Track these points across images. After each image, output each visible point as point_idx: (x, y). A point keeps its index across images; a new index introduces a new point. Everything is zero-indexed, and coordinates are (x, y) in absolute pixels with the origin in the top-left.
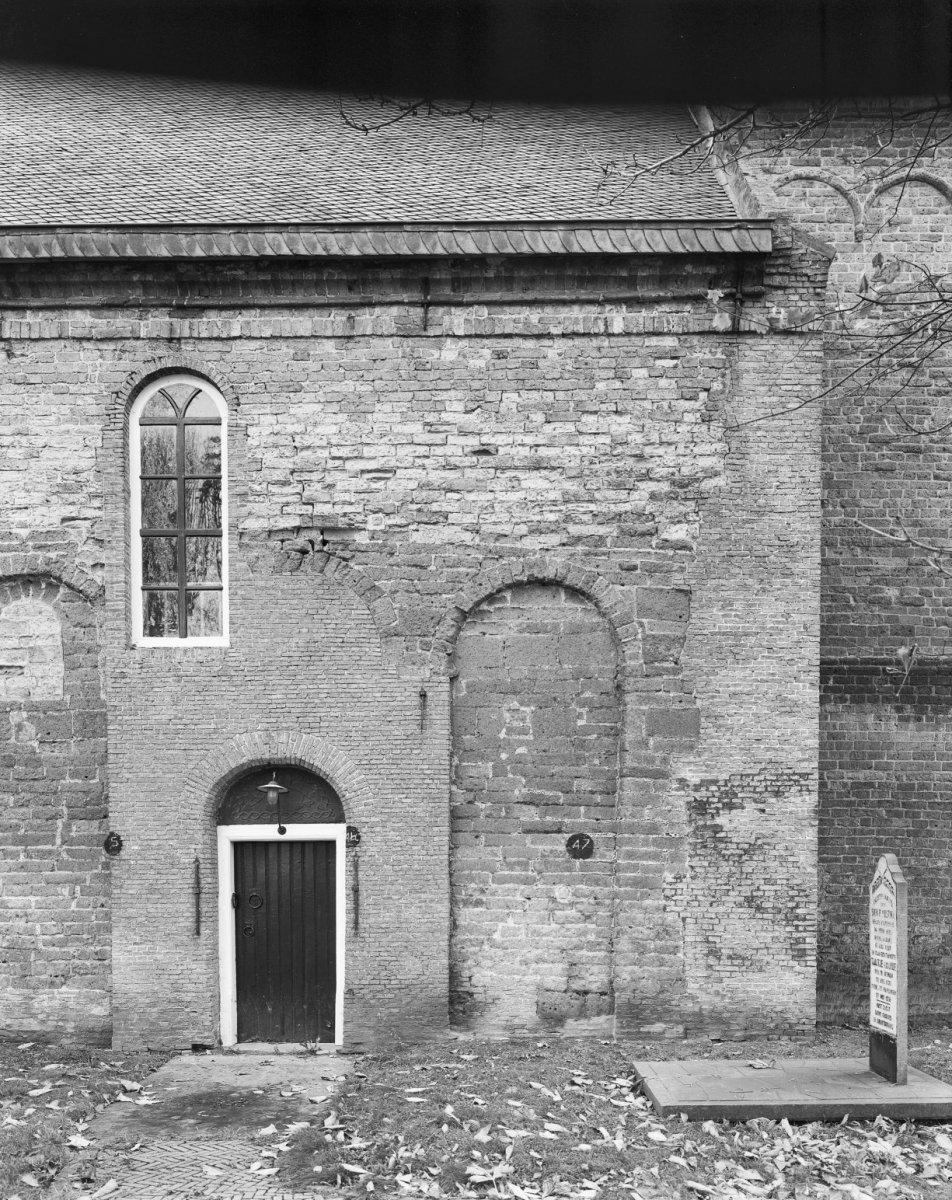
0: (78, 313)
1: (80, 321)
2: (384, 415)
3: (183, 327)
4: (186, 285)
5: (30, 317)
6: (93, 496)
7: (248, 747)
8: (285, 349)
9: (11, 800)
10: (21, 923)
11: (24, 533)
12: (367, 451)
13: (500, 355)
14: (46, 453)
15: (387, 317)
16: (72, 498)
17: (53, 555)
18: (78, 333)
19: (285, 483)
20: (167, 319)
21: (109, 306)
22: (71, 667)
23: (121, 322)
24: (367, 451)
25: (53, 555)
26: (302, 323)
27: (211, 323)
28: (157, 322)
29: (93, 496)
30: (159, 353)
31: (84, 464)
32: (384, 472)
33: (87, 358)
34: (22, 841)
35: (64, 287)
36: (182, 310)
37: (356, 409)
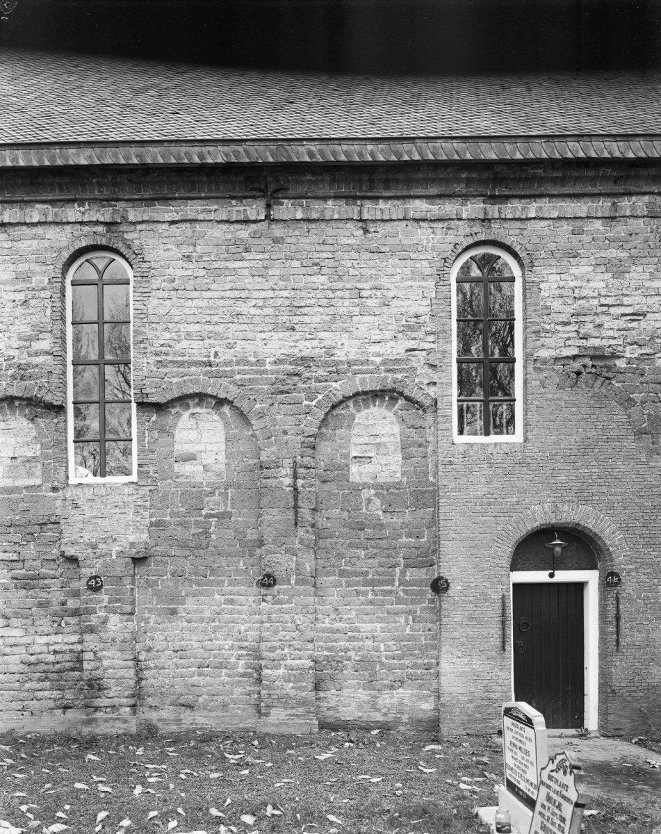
0: (417, 202)
1: (419, 207)
2: (637, 274)
3: (494, 211)
4: (498, 180)
5: (381, 204)
6: (429, 333)
7: (540, 514)
8: (566, 227)
9: (362, 553)
10: (369, 643)
11: (378, 360)
12: (626, 300)
14: (394, 303)
15: (641, 203)
16: (414, 335)
17: (399, 376)
18: (417, 216)
19: (568, 324)
20: (482, 205)
21: (440, 196)
22: (407, 457)
24: (626, 300)
25: (399, 376)
27: (513, 208)
28: (474, 208)
29: (429, 333)
30: (475, 229)
31: (422, 310)
32: (638, 315)
33: (423, 234)
34: (371, 583)
35: (409, 182)
36: (493, 199)
37: (617, 269)
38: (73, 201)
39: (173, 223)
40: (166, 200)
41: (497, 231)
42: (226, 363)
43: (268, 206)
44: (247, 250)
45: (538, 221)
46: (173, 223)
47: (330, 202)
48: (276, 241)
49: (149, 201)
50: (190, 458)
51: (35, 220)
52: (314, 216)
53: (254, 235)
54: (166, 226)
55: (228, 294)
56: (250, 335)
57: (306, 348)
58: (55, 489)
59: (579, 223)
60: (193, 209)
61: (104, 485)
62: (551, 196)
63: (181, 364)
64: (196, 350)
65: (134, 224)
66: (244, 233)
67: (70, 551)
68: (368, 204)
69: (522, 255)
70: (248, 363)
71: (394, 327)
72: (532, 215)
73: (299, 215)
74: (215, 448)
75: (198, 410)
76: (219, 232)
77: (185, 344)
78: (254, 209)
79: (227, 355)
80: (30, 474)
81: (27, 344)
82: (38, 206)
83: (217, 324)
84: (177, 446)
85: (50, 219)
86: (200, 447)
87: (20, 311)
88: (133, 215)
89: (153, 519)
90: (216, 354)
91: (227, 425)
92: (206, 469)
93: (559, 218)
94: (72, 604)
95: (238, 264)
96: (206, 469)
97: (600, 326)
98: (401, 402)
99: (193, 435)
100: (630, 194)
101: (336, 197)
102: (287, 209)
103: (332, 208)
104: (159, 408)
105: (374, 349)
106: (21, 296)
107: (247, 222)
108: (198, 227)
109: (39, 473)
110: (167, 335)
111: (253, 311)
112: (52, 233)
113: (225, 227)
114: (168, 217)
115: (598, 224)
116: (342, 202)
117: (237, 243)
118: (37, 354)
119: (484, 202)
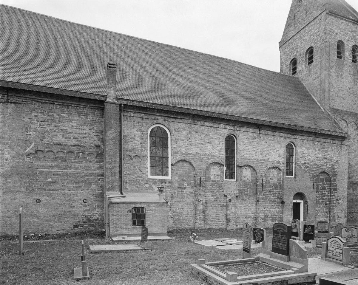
0: (281, 133)
1: (282, 134)
3: (292, 136)
4: (293, 132)
8: (301, 141)
11: (275, 161)
13: (321, 144)
14: (278, 151)
16: (281, 157)
20: (290, 135)
21: (285, 133)
23: (286, 135)
26: (304, 138)
28: (289, 136)
31: (282, 153)
35: (281, 130)
36: (292, 134)
37: (308, 149)
38: (228, 125)
39: (244, 131)
40: (243, 127)
41: (294, 141)
42: (253, 160)
43: (259, 131)
44: (256, 138)
45: (298, 140)
46: (244, 131)
48: (260, 137)
49: (240, 127)
50: (245, 177)
51: (221, 127)
52: (266, 134)
53: (257, 135)
54: (243, 132)
55: (253, 146)
57: (265, 158)
58: (222, 181)
60: (248, 129)
61: (230, 181)
63: (245, 159)
64: (247, 156)
65: (238, 130)
66: (255, 135)
67: (226, 194)
68: (274, 133)
69: (296, 145)
70: (256, 160)
71: (278, 156)
72: (297, 138)
73: (264, 133)
74: (249, 175)
75: (247, 168)
76: (251, 134)
77: (246, 155)
78: (257, 131)
79: (252, 158)
80: (218, 178)
81: (219, 152)
82: (221, 125)
85: (224, 127)
87: (218, 145)
88: (238, 129)
89: (239, 188)
90: (251, 158)
91: (251, 171)
92: (248, 179)
94: (225, 204)
95: (254, 141)
96: (248, 179)
97: (306, 158)
98: (277, 169)
99: (246, 172)
100: (310, 137)
102: (262, 131)
103: (269, 132)
104: (240, 167)
106: (218, 142)
107: (256, 133)
108: (248, 133)
109: (219, 178)
110: (243, 153)
111: (257, 150)
112: (224, 130)
113: (252, 133)
114: (244, 130)
115: (306, 141)
116: (270, 132)
117: (254, 137)
118: (221, 154)
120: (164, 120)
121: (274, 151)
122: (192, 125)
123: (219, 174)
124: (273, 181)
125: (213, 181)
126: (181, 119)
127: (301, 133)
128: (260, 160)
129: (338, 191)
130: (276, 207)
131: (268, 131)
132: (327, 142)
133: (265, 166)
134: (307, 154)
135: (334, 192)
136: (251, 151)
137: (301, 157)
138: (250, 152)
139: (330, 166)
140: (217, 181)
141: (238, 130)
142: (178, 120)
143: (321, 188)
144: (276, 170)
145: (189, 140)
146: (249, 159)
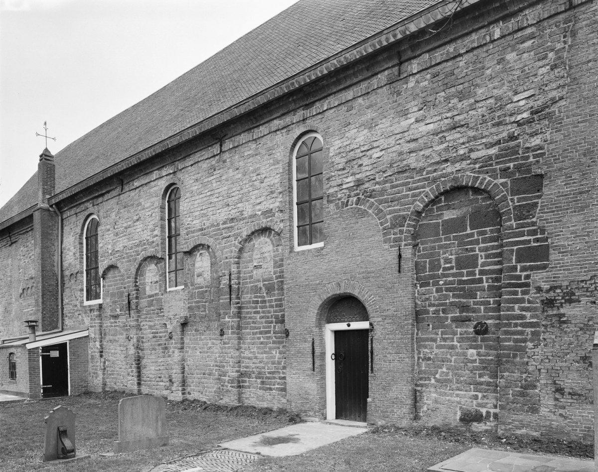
4: (307, 95)
5: (261, 128)
11: (259, 213)
14: (266, 180)
16: (274, 195)
21: (283, 115)
23: (288, 119)
26: (349, 94)
33: (279, 138)
35: (271, 113)
36: (308, 106)
37: (371, 125)
39: (192, 165)
42: (208, 227)
46: (192, 165)
47: (242, 135)
54: (190, 168)
56: (214, 212)
57: (234, 213)
59: (350, 104)
60: (197, 157)
62: (335, 93)
66: (213, 161)
78: (216, 149)
83: (204, 209)
84: (196, 270)
86: (203, 269)
93: (339, 105)
100: (377, 74)
101: (244, 132)
102: (228, 145)
103: (243, 138)
105: (258, 207)
108: (200, 164)
116: (246, 133)
119: (303, 110)
120: (93, 206)
121: (255, 183)
122: (121, 196)
123: (158, 280)
124: (260, 271)
125: (150, 296)
126: (108, 192)
127: (339, 82)
128: (224, 223)
129: (554, 256)
130: (270, 349)
131: (240, 134)
132: (462, 51)
133: (236, 236)
134: (366, 148)
135: (524, 269)
136: (204, 207)
137: (340, 166)
138: (202, 210)
139: (493, 151)
140: (156, 294)
141: (181, 170)
142: (106, 197)
143: (447, 261)
144: (269, 237)
145: (116, 227)
146: (202, 230)
